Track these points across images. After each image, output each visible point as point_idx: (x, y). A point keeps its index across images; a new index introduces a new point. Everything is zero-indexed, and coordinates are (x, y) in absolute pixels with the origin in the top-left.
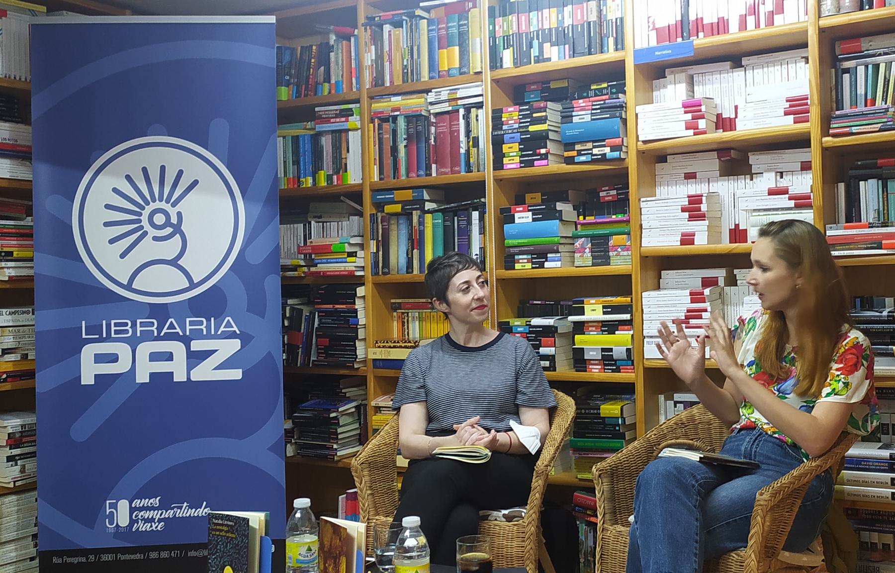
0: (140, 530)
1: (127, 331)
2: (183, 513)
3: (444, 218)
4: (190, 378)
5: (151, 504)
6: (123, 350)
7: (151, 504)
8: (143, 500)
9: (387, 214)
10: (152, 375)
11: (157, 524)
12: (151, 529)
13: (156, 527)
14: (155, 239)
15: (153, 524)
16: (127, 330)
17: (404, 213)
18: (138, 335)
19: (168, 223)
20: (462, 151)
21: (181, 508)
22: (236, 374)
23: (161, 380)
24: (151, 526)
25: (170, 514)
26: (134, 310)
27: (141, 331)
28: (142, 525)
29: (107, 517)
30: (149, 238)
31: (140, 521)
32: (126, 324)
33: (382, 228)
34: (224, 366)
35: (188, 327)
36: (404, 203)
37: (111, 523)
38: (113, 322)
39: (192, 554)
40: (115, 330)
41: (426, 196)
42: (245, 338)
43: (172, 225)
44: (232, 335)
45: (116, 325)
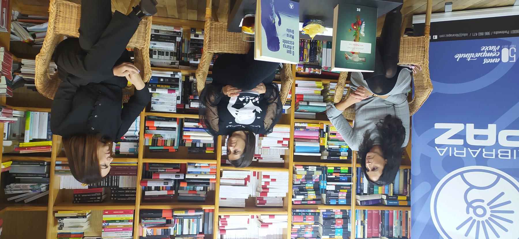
0: (495, 46)
1: (501, 152)
2: (470, 55)
3: (373, 191)
4: (464, 125)
5: (488, 60)
6: (503, 142)
7: (488, 60)
8: (493, 62)
9: (406, 196)
10: (486, 127)
11: (485, 50)
12: (489, 47)
13: (486, 48)
14: (483, 201)
15: (488, 50)
16: (501, 153)
17: (397, 195)
18: (494, 150)
19: (475, 209)
20: (366, 220)
21: (471, 58)
22: (438, 126)
23: (481, 125)
24: (489, 48)
25: (478, 55)
26: (497, 163)
27: (493, 152)
28: (494, 49)
29: (515, 53)
30: (487, 201)
31: (495, 51)
32: (501, 156)
33: (407, 189)
34: (443, 131)
35: (465, 152)
36: (396, 200)
37: (513, 50)
38: (510, 158)
39: (465, 35)
40: (508, 153)
41: (386, 202)
42: (432, 144)
43: (473, 207)
44: (439, 146)
45: (508, 156)
